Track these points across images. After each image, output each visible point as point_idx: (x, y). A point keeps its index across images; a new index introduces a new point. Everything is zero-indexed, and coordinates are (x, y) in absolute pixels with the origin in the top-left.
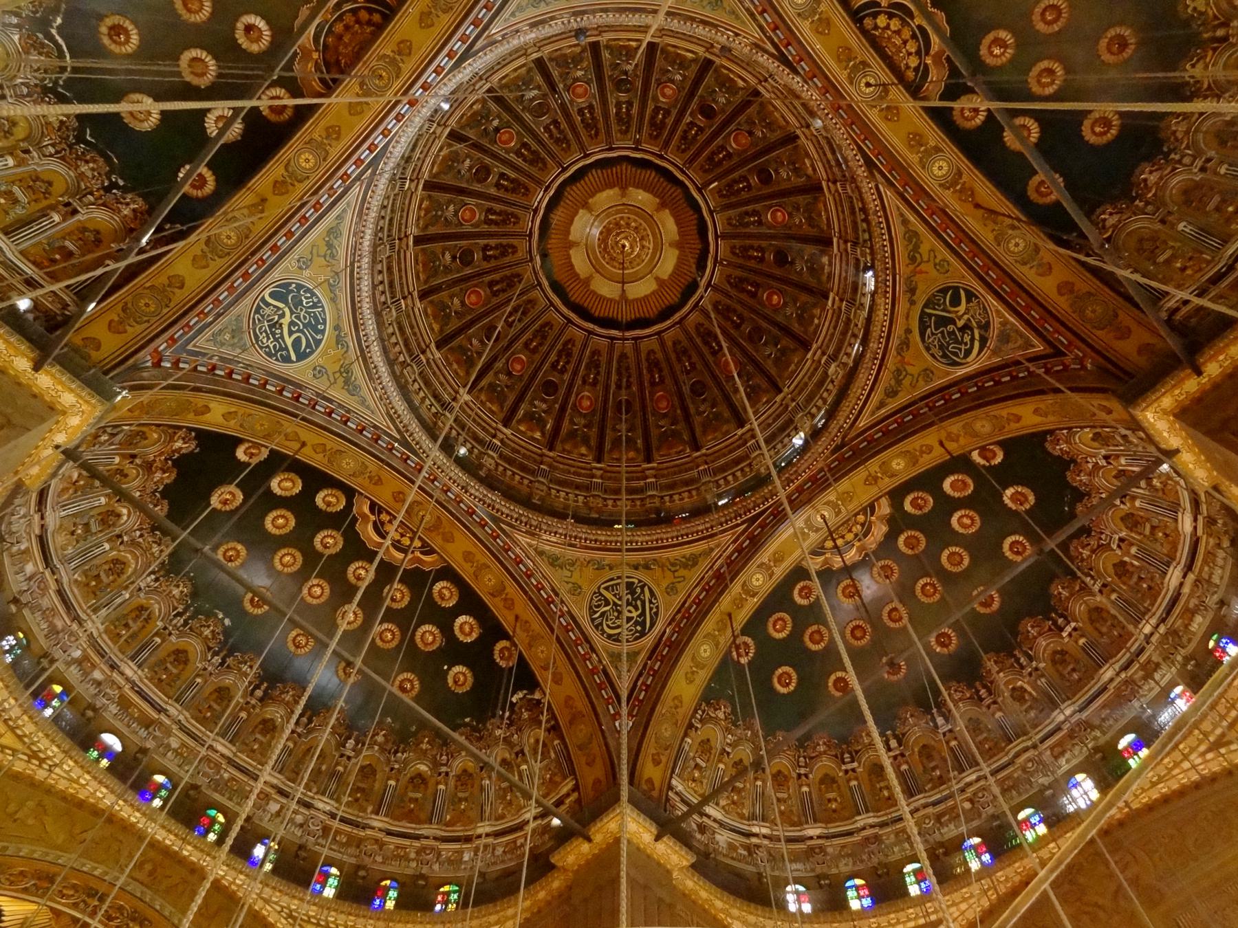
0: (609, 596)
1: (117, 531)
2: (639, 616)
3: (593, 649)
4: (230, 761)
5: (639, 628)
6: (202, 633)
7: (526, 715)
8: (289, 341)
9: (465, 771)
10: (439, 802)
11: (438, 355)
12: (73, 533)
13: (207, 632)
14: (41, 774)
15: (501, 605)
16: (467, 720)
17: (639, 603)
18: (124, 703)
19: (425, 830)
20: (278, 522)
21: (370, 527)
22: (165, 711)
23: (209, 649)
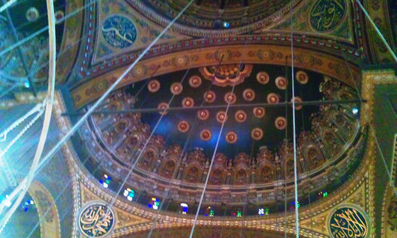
0: (317, 14)
1: (139, 143)
2: (336, 8)
3: (327, 39)
4: (232, 191)
5: (339, 13)
6: (195, 158)
7: (329, 92)
8: (125, 38)
9: (327, 134)
10: (324, 152)
11: (199, 7)
12: (125, 152)
13: (197, 157)
14: (162, 226)
15: (278, 59)
16: (312, 115)
17: (331, 4)
18: (180, 192)
19: (325, 166)
20: (187, 103)
21: (216, 79)
22: (198, 188)
23: (202, 161)
